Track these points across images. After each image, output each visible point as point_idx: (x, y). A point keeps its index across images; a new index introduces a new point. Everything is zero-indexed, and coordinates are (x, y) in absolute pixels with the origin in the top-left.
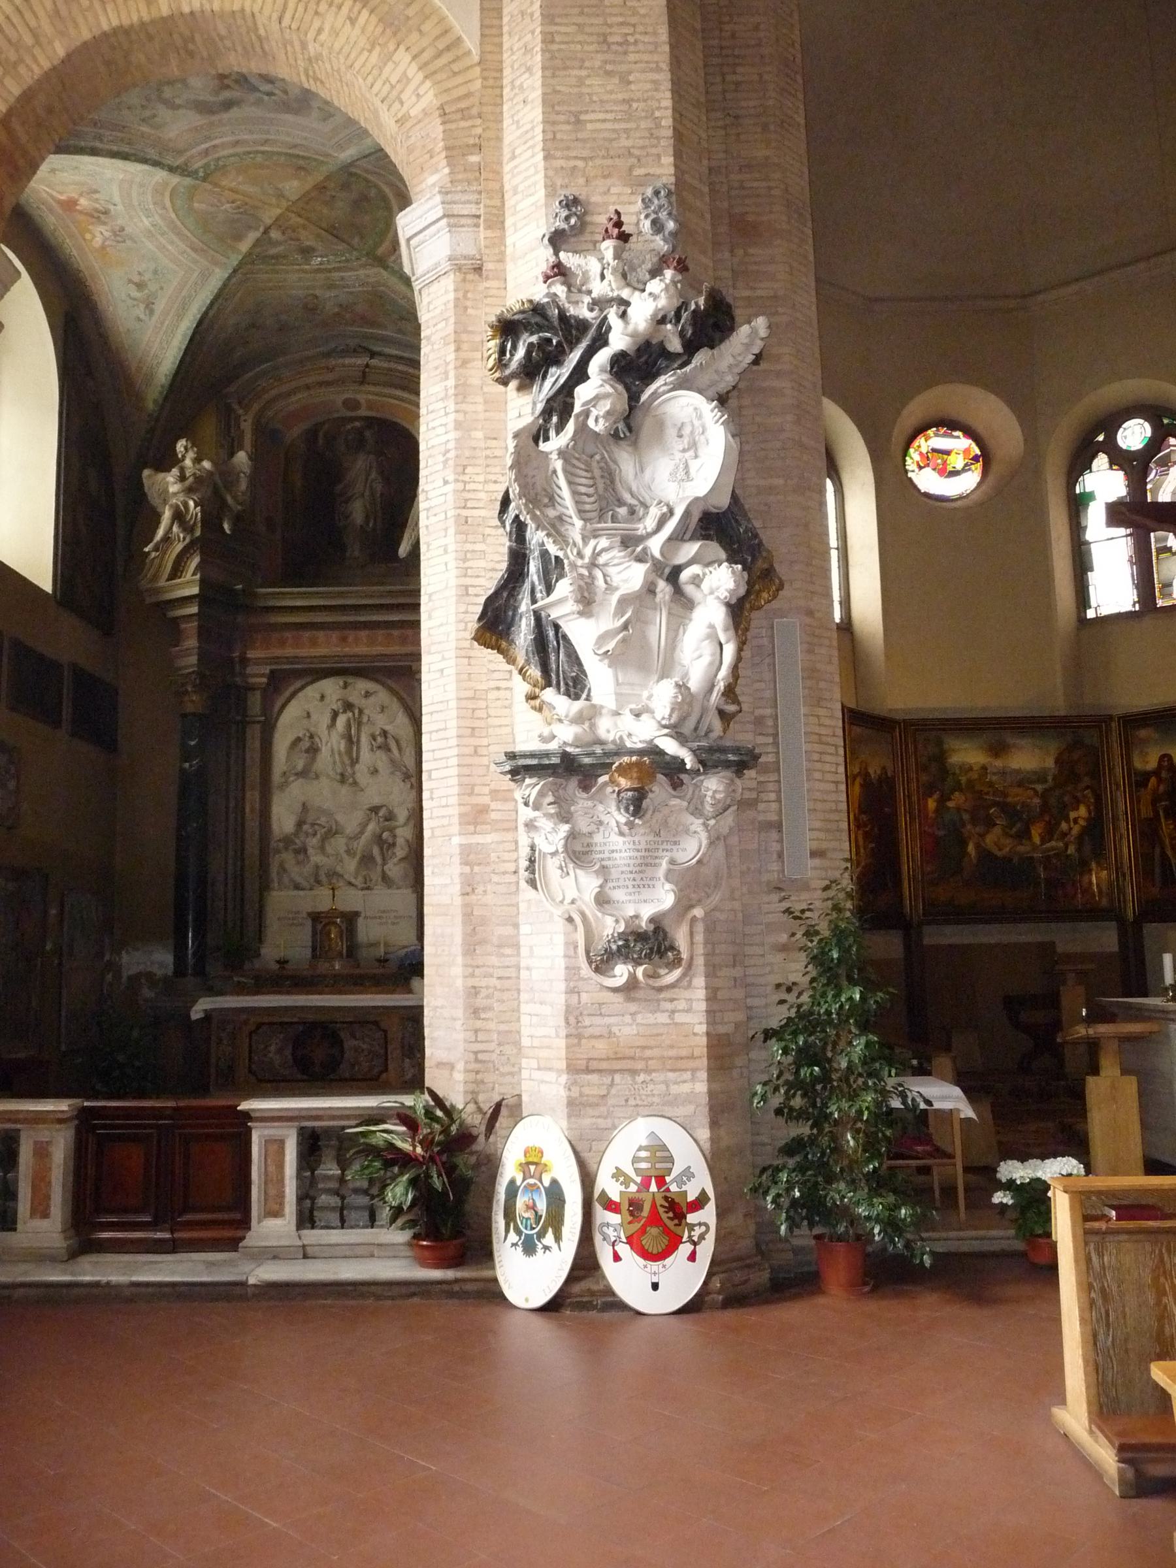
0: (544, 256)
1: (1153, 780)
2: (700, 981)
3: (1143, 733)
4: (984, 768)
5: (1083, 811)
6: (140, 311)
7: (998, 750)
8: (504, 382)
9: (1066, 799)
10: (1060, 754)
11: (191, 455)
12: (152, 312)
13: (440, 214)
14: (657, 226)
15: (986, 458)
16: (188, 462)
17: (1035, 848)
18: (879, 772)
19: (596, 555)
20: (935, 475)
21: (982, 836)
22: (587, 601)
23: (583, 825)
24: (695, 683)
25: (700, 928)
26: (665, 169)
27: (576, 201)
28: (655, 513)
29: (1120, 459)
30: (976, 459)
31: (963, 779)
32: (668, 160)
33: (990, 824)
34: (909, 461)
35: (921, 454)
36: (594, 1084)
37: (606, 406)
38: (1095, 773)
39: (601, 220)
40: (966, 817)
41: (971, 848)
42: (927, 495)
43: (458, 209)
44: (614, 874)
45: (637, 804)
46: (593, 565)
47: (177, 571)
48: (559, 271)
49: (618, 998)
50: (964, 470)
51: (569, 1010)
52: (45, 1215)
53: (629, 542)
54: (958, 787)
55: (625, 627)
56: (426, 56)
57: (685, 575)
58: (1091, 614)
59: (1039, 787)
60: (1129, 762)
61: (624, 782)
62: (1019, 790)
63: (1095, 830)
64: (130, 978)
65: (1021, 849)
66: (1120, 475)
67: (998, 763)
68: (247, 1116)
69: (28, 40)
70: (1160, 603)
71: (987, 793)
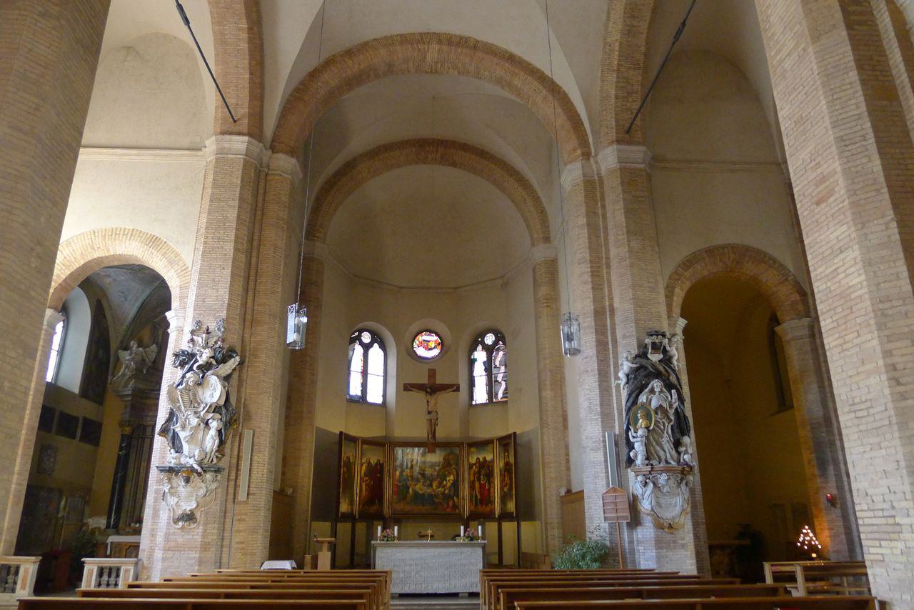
0: (189, 336)
1: (474, 467)
2: (201, 527)
3: (472, 449)
5: (452, 477)
6: (123, 299)
8: (176, 367)
9: (446, 473)
10: (445, 456)
11: (135, 346)
12: (126, 300)
13: (174, 315)
14: (219, 329)
15: (442, 344)
16: (134, 349)
17: (434, 491)
18: (376, 461)
19: (188, 415)
20: (424, 349)
21: (415, 485)
22: (183, 428)
23: (175, 485)
24: (208, 450)
25: (203, 513)
26: (224, 314)
27: (200, 322)
28: (203, 406)
29: (486, 348)
30: (439, 344)
32: (225, 312)
34: (415, 344)
36: (170, 554)
37: (192, 379)
38: (457, 464)
39: (205, 327)
41: (410, 490)
42: (420, 357)
43: (179, 314)
44: (182, 498)
45: (187, 480)
46: (187, 418)
47: (126, 386)
48: (192, 340)
49: (180, 531)
50: (434, 348)
51: (166, 533)
52: (24, 589)
53: (196, 413)
55: (192, 435)
56: (179, 271)
57: (210, 421)
58: (474, 403)
60: (468, 460)
61: (184, 475)
63: (456, 485)
64: (92, 529)
65: (429, 491)
66: (485, 353)
68: (84, 562)
69: (73, 260)
70: (494, 401)
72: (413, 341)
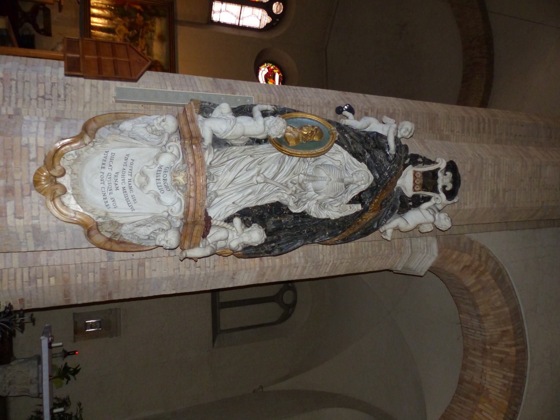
4: (153, 31)
7: (161, 38)
10: (159, 63)
31: (149, 22)
33: (130, 29)
35: (273, 69)
40: (133, 20)
54: (145, 19)
59: (145, 52)
62: (144, 43)
67: (155, 37)
71: (143, 31)
72: (273, 63)
